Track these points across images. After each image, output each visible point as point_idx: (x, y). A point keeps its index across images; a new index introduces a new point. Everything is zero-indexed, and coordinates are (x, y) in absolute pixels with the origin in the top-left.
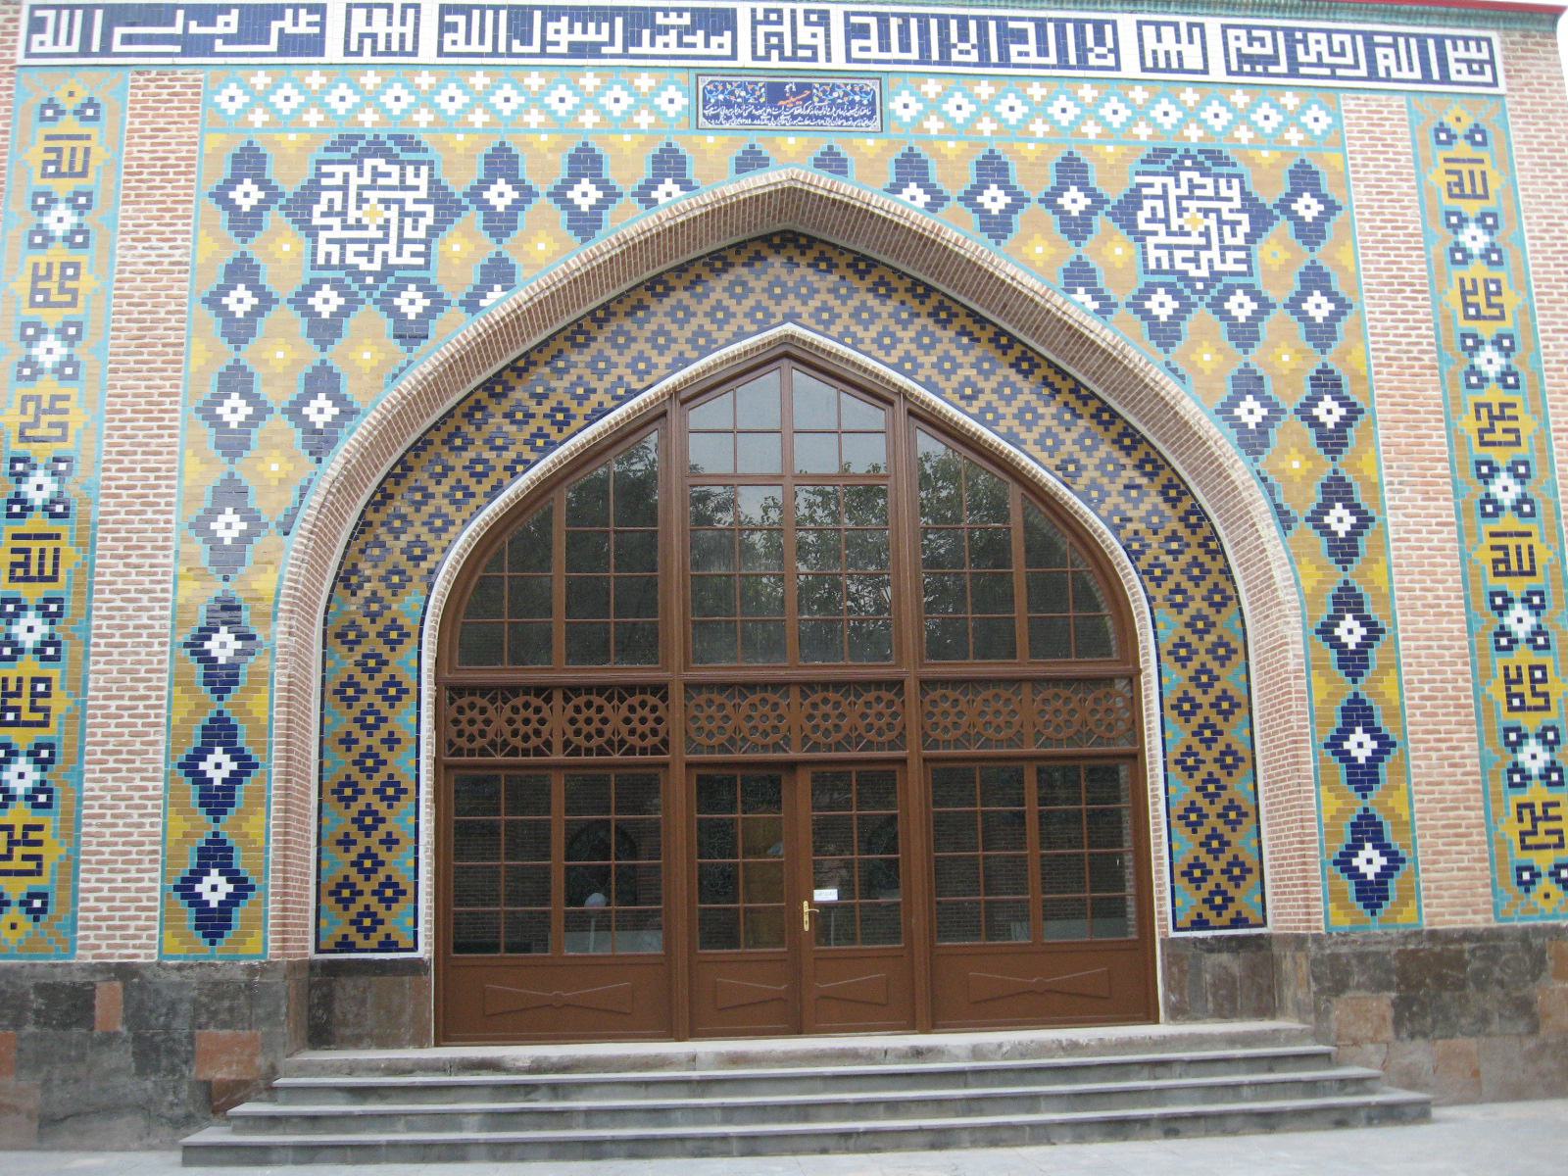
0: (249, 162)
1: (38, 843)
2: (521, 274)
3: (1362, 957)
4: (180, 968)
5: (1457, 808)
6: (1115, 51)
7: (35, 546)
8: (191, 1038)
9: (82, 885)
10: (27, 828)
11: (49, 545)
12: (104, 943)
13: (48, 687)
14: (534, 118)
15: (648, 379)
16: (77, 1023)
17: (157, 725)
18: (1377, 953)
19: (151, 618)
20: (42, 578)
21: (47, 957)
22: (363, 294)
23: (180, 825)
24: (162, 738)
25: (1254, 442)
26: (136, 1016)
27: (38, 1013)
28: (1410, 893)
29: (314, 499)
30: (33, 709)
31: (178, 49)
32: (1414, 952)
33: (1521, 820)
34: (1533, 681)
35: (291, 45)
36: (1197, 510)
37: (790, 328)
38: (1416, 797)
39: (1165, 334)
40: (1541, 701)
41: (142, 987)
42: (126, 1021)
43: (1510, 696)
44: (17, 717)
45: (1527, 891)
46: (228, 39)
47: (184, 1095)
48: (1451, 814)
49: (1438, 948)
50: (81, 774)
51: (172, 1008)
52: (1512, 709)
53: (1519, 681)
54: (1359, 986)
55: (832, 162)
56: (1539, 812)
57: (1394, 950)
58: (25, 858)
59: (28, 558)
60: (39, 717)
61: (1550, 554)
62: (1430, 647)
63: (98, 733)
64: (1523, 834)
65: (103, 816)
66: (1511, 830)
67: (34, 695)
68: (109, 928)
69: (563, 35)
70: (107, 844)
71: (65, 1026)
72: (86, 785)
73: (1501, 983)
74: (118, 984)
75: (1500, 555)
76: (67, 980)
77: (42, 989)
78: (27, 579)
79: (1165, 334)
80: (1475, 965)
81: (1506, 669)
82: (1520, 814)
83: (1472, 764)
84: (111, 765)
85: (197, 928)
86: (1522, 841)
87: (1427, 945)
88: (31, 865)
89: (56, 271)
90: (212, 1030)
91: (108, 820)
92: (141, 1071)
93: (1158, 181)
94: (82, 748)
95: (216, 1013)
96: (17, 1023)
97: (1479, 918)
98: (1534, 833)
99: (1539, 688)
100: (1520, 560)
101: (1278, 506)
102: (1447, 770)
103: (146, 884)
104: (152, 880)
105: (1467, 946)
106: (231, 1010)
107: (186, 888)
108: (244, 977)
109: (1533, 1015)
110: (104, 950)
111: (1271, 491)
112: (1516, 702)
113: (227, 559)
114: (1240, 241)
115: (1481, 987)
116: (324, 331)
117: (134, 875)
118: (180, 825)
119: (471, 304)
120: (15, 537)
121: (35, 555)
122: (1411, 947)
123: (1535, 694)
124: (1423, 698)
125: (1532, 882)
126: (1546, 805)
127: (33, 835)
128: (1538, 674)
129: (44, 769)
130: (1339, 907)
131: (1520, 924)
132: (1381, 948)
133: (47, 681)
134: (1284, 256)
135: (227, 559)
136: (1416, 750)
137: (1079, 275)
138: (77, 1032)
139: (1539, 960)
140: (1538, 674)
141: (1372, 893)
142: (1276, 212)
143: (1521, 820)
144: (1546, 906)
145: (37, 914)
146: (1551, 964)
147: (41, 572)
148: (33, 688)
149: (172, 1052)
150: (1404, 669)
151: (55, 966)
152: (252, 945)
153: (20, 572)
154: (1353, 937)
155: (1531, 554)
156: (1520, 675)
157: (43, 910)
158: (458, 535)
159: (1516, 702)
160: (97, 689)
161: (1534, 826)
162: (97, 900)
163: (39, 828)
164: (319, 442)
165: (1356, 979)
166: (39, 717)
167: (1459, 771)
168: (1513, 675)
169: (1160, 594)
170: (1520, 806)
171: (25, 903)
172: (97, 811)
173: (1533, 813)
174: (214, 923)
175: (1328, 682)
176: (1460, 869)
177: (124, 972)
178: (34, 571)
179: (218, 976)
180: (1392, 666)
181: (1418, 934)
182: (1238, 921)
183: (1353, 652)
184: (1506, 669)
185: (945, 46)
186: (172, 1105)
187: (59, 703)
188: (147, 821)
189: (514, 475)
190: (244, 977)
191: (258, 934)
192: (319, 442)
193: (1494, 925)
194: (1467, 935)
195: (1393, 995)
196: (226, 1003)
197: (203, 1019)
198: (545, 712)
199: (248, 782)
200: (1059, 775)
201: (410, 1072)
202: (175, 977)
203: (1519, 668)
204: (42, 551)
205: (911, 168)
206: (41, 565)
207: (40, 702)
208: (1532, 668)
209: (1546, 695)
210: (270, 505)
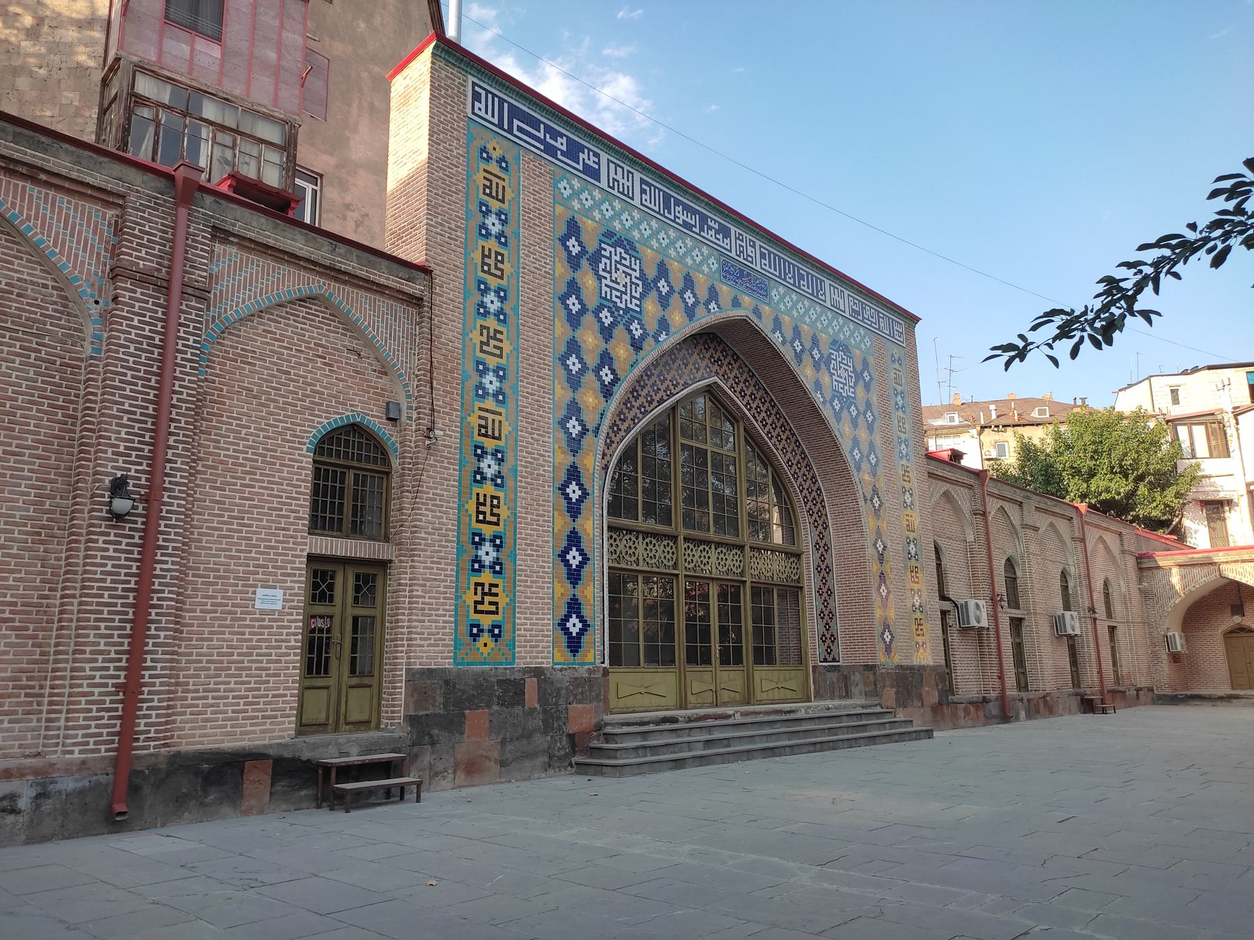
0: (573, 228)
1: (496, 595)
2: (672, 329)
3: (888, 674)
4: (561, 670)
7: (490, 416)
8: (567, 709)
9: (517, 621)
10: (491, 585)
11: (497, 418)
12: (528, 655)
13: (499, 502)
14: (672, 252)
15: (677, 390)
16: (518, 703)
17: (548, 531)
19: (544, 470)
20: (494, 438)
21: (501, 664)
22: (619, 319)
23: (559, 590)
24: (551, 539)
26: (543, 699)
27: (499, 698)
29: (606, 423)
30: (492, 514)
31: (542, 147)
35: (588, 170)
36: (819, 489)
37: (715, 379)
41: (545, 680)
42: (539, 700)
44: (485, 517)
46: (563, 153)
47: (564, 743)
50: (515, 555)
51: (558, 696)
55: (757, 312)
58: (491, 603)
59: (487, 423)
60: (494, 519)
63: (523, 532)
65: (527, 581)
67: (492, 506)
68: (531, 647)
69: (683, 217)
70: (529, 598)
71: (512, 705)
72: (518, 562)
74: (535, 679)
76: (512, 678)
77: (500, 682)
78: (486, 435)
84: (529, 552)
85: (568, 647)
88: (493, 608)
89: (493, 255)
90: (575, 705)
91: (529, 584)
92: (545, 733)
94: (515, 540)
95: (575, 696)
96: (489, 706)
103: (546, 622)
104: (549, 619)
106: (582, 693)
107: (563, 624)
108: (587, 675)
110: (528, 660)
113: (574, 444)
116: (607, 332)
117: (540, 616)
118: (559, 590)
120: (480, 409)
121: (490, 422)
127: (494, 590)
129: (498, 551)
133: (498, 498)
135: (574, 444)
137: (818, 385)
138: (518, 710)
145: (496, 637)
147: (493, 433)
148: (492, 502)
149: (559, 718)
151: (506, 669)
152: (590, 658)
153: (483, 431)
157: (499, 635)
158: (616, 448)
160: (522, 508)
162: (525, 630)
163: (497, 586)
164: (607, 392)
165: (887, 683)
166: (494, 519)
169: (812, 521)
171: (491, 631)
172: (523, 578)
174: (574, 644)
177: (538, 672)
178: (490, 433)
179: (577, 675)
182: (834, 660)
185: (786, 274)
186: (559, 749)
187: (504, 512)
188: (546, 585)
189: (635, 424)
190: (587, 675)
191: (592, 650)
192: (607, 392)
196: (580, 690)
197: (571, 699)
198: (636, 545)
199: (586, 568)
201: (647, 723)
202: (559, 675)
204: (493, 420)
205: (777, 325)
206: (493, 429)
207: (495, 510)
210: (591, 420)
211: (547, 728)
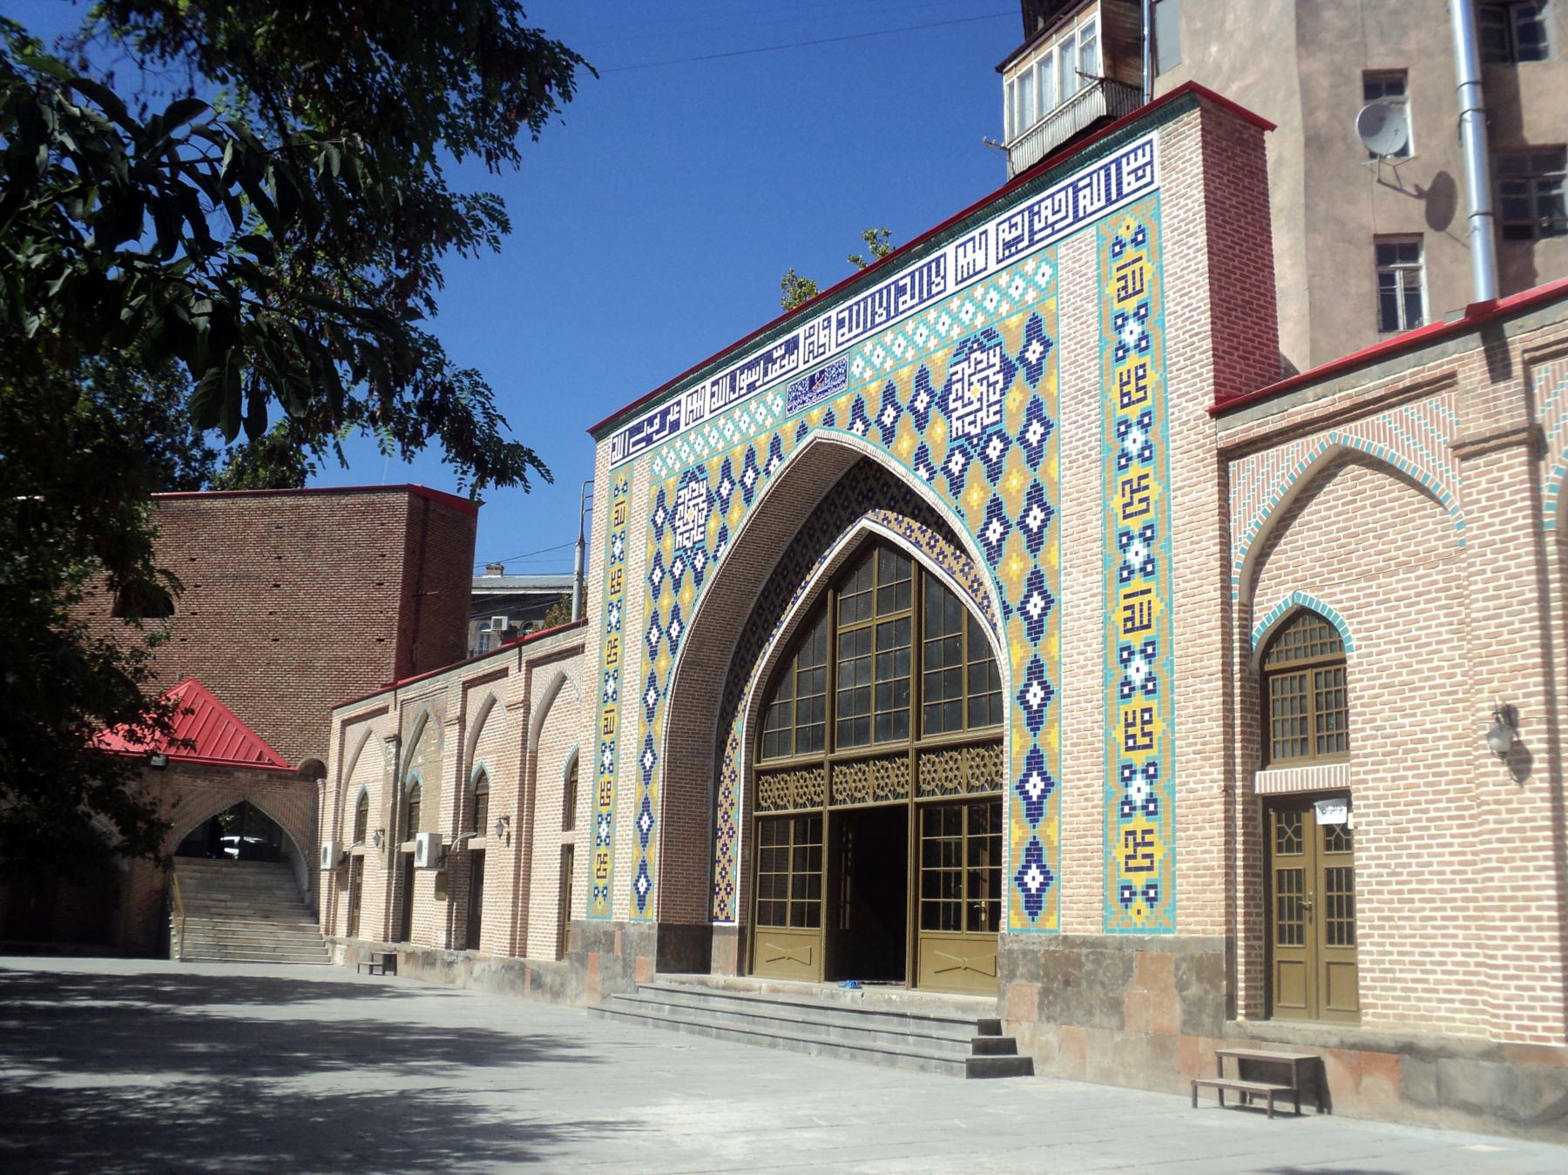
3: (1025, 953)
5: (1086, 836)
6: (944, 277)
18: (1033, 951)
25: (994, 553)
28: (1056, 906)
32: (1054, 952)
33: (1127, 846)
34: (1144, 723)
38: (1063, 827)
39: (956, 485)
40: (1146, 741)
43: (1128, 737)
45: (1127, 907)
48: (1083, 840)
49: (1067, 951)
52: (1128, 749)
53: (1133, 724)
54: (1022, 975)
56: (1139, 840)
57: (1043, 948)
61: (1162, 606)
62: (1079, 702)
64: (1128, 857)
66: (1120, 854)
73: (1103, 984)
75: (1128, 614)
79: (956, 485)
80: (1089, 966)
81: (1126, 713)
82: (1126, 840)
83: (1098, 799)
86: (1127, 863)
87: (1061, 948)
93: (958, 368)
97: (1093, 928)
98: (1133, 857)
99: (1147, 728)
100: (1141, 616)
101: (1004, 602)
102: (1083, 804)
105: (1084, 951)
109: (1121, 1014)
111: (1000, 588)
112: (1131, 743)
114: (997, 397)
115: (1090, 983)
119: (715, 558)
122: (1052, 948)
123: (1144, 735)
124: (1073, 745)
125: (1129, 900)
126: (1145, 832)
128: (1146, 716)
130: (1016, 914)
131: (1118, 935)
132: (1036, 948)
134: (1019, 397)
136: (1065, 788)
139: (1128, 969)
140: (1146, 716)
141: (1034, 904)
142: (1017, 364)
143: (1127, 846)
144: (1137, 919)
146: (1136, 971)
150: (1063, 722)
154: (1023, 937)
155: (1149, 608)
156: (1134, 718)
159: (1131, 743)
161: (1135, 851)
165: (1021, 970)
167: (1090, 804)
168: (1130, 720)
170: (1128, 833)
173: (1135, 839)
175: (1021, 737)
176: (1085, 887)
180: (1056, 720)
181: (1056, 938)
183: (1036, 712)
184: (1126, 713)
193: (1105, 934)
194: (1085, 942)
195: (1040, 985)
200: (939, 816)
203: (1134, 712)
208: (1144, 711)
209: (1150, 734)
211: (624, 975)
